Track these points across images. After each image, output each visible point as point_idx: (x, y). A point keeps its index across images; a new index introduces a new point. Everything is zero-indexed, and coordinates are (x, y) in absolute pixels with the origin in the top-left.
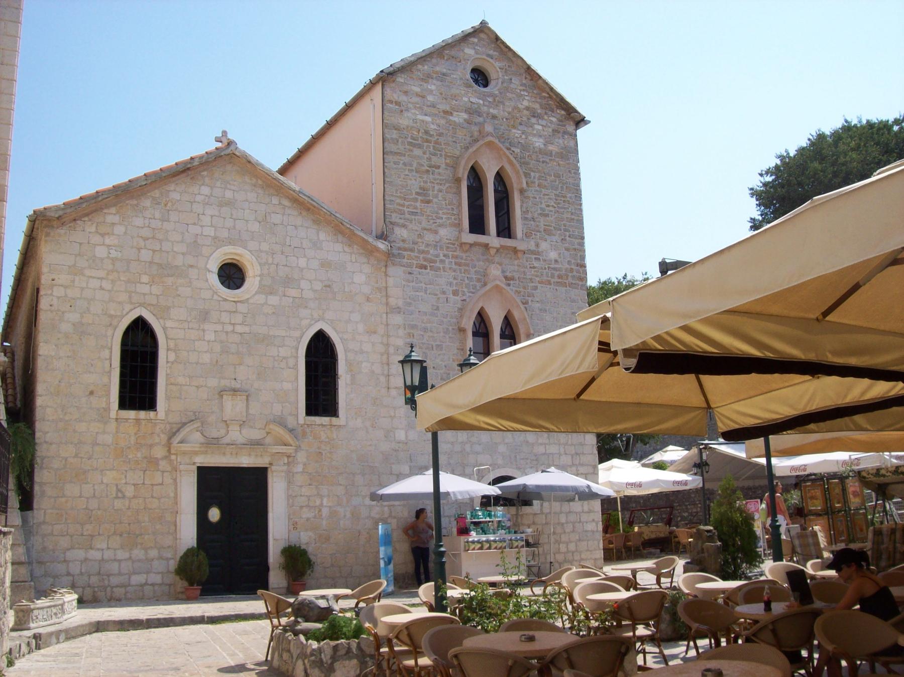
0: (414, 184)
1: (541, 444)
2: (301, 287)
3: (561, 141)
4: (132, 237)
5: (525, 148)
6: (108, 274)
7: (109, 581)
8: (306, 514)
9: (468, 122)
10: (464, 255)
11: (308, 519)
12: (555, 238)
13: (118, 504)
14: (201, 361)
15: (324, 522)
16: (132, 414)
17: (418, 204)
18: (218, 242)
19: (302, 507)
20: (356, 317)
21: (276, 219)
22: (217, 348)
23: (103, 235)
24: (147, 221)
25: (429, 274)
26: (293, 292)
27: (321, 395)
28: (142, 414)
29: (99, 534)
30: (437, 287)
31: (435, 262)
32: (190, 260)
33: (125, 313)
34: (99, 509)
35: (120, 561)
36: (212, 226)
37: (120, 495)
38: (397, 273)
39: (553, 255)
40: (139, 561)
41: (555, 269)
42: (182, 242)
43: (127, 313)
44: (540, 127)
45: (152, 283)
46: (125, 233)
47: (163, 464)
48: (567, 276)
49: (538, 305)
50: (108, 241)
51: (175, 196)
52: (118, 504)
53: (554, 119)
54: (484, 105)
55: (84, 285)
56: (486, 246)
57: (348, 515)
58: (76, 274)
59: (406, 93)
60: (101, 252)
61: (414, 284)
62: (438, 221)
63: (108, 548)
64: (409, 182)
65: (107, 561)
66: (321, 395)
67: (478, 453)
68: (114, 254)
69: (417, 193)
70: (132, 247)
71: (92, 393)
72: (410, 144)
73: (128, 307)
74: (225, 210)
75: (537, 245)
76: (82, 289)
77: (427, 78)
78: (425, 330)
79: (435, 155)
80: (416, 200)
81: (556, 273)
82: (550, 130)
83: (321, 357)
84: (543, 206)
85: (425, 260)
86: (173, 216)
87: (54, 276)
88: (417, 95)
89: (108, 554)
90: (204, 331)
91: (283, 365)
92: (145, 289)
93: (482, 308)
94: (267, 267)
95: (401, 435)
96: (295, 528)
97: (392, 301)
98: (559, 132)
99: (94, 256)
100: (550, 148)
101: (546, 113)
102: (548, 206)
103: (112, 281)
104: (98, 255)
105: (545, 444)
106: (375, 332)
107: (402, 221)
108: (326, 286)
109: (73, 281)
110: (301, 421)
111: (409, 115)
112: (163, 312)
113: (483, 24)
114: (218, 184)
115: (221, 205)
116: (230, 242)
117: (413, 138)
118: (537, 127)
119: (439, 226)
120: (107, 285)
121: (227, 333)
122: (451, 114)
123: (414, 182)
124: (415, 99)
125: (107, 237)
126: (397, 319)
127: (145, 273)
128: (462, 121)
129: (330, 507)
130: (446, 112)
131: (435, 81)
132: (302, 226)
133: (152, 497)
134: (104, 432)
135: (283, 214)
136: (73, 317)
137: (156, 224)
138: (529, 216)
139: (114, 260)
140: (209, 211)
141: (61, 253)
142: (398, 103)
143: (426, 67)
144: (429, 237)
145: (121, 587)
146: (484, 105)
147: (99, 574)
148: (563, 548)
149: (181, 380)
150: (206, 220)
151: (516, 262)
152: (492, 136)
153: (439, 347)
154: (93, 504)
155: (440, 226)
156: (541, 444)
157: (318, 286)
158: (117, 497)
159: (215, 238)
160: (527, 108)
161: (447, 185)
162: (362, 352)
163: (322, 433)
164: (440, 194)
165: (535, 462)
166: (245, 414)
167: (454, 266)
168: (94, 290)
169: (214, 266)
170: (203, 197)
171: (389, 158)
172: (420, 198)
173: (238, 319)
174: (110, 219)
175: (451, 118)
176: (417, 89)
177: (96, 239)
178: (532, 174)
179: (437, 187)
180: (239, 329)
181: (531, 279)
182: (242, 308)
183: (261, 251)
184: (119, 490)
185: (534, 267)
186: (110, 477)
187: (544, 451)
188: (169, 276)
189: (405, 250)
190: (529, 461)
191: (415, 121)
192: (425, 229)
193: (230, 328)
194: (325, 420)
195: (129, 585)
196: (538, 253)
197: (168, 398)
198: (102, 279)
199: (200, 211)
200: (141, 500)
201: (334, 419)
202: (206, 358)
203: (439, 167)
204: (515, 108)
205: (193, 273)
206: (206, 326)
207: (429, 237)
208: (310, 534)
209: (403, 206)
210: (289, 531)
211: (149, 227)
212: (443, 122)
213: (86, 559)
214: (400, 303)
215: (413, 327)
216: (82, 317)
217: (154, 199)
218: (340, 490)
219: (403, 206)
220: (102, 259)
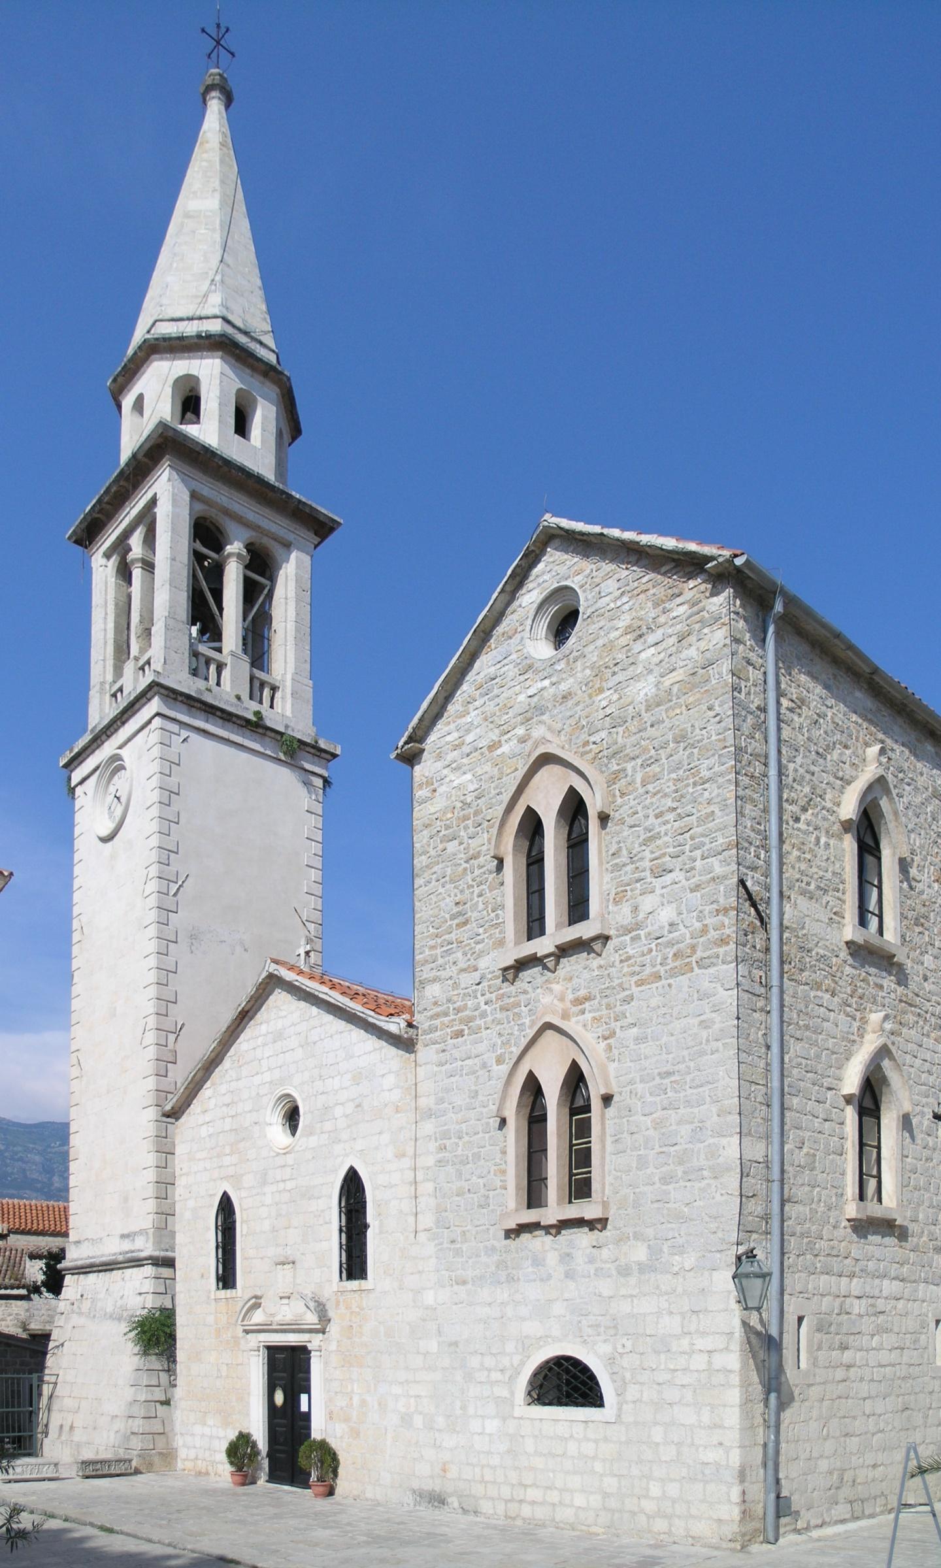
8: (341, 1402)
39: (666, 914)
49: (635, 1030)
59: (439, 757)
62: (480, 946)
64: (442, 904)
75: (635, 909)
81: (670, 952)
85: (461, 1021)
105: (632, 1296)
107: (434, 973)
119: (479, 956)
123: (448, 900)
138: (624, 858)
142: (429, 783)
144: (467, 979)
164: (481, 899)
165: (612, 1332)
181: (620, 985)
185: (628, 958)
187: (628, 1311)
189: (437, 1015)
190: (602, 1329)
192: (463, 970)
212: (487, 767)
219: (432, 948)
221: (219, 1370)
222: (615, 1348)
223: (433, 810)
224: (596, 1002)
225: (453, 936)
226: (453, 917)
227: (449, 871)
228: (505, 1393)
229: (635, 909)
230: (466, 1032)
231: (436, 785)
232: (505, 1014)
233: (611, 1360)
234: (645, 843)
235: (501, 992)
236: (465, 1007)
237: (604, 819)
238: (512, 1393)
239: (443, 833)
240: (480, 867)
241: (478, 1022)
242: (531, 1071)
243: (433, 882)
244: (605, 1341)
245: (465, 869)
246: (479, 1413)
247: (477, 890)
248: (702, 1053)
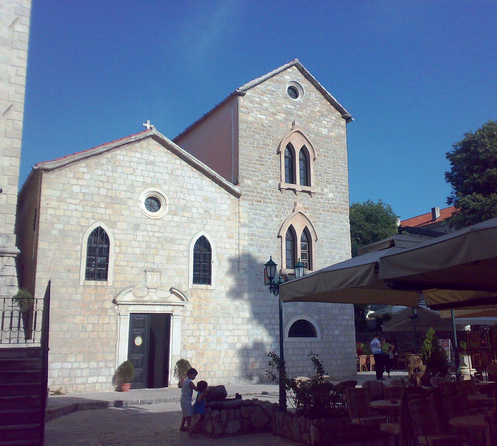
0: (256, 154)
2: (192, 211)
3: (337, 131)
4: (95, 181)
5: (317, 134)
6: (80, 202)
7: (75, 380)
8: (192, 340)
9: (285, 119)
11: (192, 344)
12: (332, 186)
13: (82, 335)
14: (134, 252)
15: (201, 345)
16: (93, 283)
17: (257, 166)
18: (145, 185)
19: (189, 336)
20: (222, 229)
21: (178, 172)
22: (144, 245)
23: (78, 179)
24: (104, 172)
25: (262, 206)
27: (202, 273)
28: (99, 283)
29: (70, 353)
30: (267, 213)
32: (129, 195)
33: (90, 224)
34: (71, 338)
35: (82, 369)
36: (142, 176)
37: (84, 330)
38: (244, 204)
39: (331, 195)
40: (94, 369)
41: (332, 204)
42: (124, 184)
43: (92, 225)
44: (326, 122)
45: (106, 208)
46: (91, 179)
47: (110, 312)
48: (339, 208)
50: (81, 182)
52: (82, 335)
53: (334, 118)
54: (295, 109)
55: (66, 208)
56: (294, 190)
57: (215, 341)
58: (61, 201)
59: (251, 102)
60: (76, 189)
61: (254, 211)
63: (76, 361)
65: (74, 369)
66: (202, 273)
68: (84, 190)
69: (257, 160)
70: (95, 187)
71: (69, 271)
72: (253, 131)
73: (92, 221)
74: (150, 167)
75: (322, 190)
76: (65, 210)
77: (264, 93)
78: (260, 237)
80: (256, 164)
83: (203, 251)
84: (326, 168)
85: (260, 197)
86: (120, 169)
87: (48, 202)
88: (258, 104)
89: (75, 365)
90: (136, 235)
91: (181, 255)
92: (102, 211)
93: (291, 225)
94: (173, 200)
96: (184, 349)
97: (242, 220)
98: (336, 125)
99: (72, 191)
100: (331, 134)
101: (329, 114)
102: (329, 168)
103: (83, 205)
104: (74, 191)
106: (232, 238)
107: (248, 176)
108: (205, 211)
109: (59, 206)
110: (190, 287)
111: (253, 114)
112: (113, 224)
114: (145, 152)
115: (147, 164)
116: (153, 185)
117: (254, 128)
118: (324, 122)
120: (80, 208)
121: (150, 236)
124: (256, 106)
125: (80, 180)
126: (245, 230)
127: (103, 202)
128: (282, 118)
129: (205, 336)
131: (267, 95)
132: (193, 177)
133: (103, 331)
134: (76, 293)
135: (183, 170)
136: (60, 226)
137: (109, 173)
139: (84, 194)
140: (141, 167)
141: (53, 189)
142: (246, 108)
144: (263, 185)
145: (82, 384)
146: (295, 109)
147: (69, 377)
148: (334, 364)
149: (123, 263)
150: (138, 172)
152: (299, 127)
153: (267, 246)
154: (68, 336)
155: (270, 178)
157: (202, 211)
158: (82, 331)
159: (144, 182)
160: (319, 111)
161: (273, 155)
162: (225, 248)
163: (202, 294)
166: (158, 283)
167: (276, 201)
168: (72, 211)
169: (143, 198)
170: (136, 159)
173: (157, 229)
174: (82, 170)
177: (74, 181)
178: (321, 149)
179: (267, 157)
180: (157, 235)
182: (159, 223)
183: (170, 191)
184: (83, 327)
185: (320, 202)
186: (78, 319)
188: (116, 204)
189: (249, 191)
191: (256, 118)
193: (151, 234)
194: (204, 286)
195: (87, 383)
196: (323, 195)
197: (115, 273)
198: (76, 205)
199: (135, 167)
200: (96, 333)
201: (209, 285)
202: (137, 251)
203: (268, 145)
204: (312, 111)
205: (131, 203)
206: (138, 233)
208: (193, 352)
209: (249, 167)
210: (181, 351)
211: (105, 175)
212: (272, 119)
213: (62, 368)
214: (246, 221)
215: (253, 235)
216: (64, 226)
217: (108, 159)
218: (211, 327)
219: (249, 167)
220: (77, 193)
222: (320, 318)
225: (257, 166)
226: (257, 160)
227: (256, 144)
229: (322, 190)
233: (319, 322)
234: (325, 173)
236: (262, 193)
239: (253, 129)
240: (269, 149)
243: (248, 144)
248: (341, 237)
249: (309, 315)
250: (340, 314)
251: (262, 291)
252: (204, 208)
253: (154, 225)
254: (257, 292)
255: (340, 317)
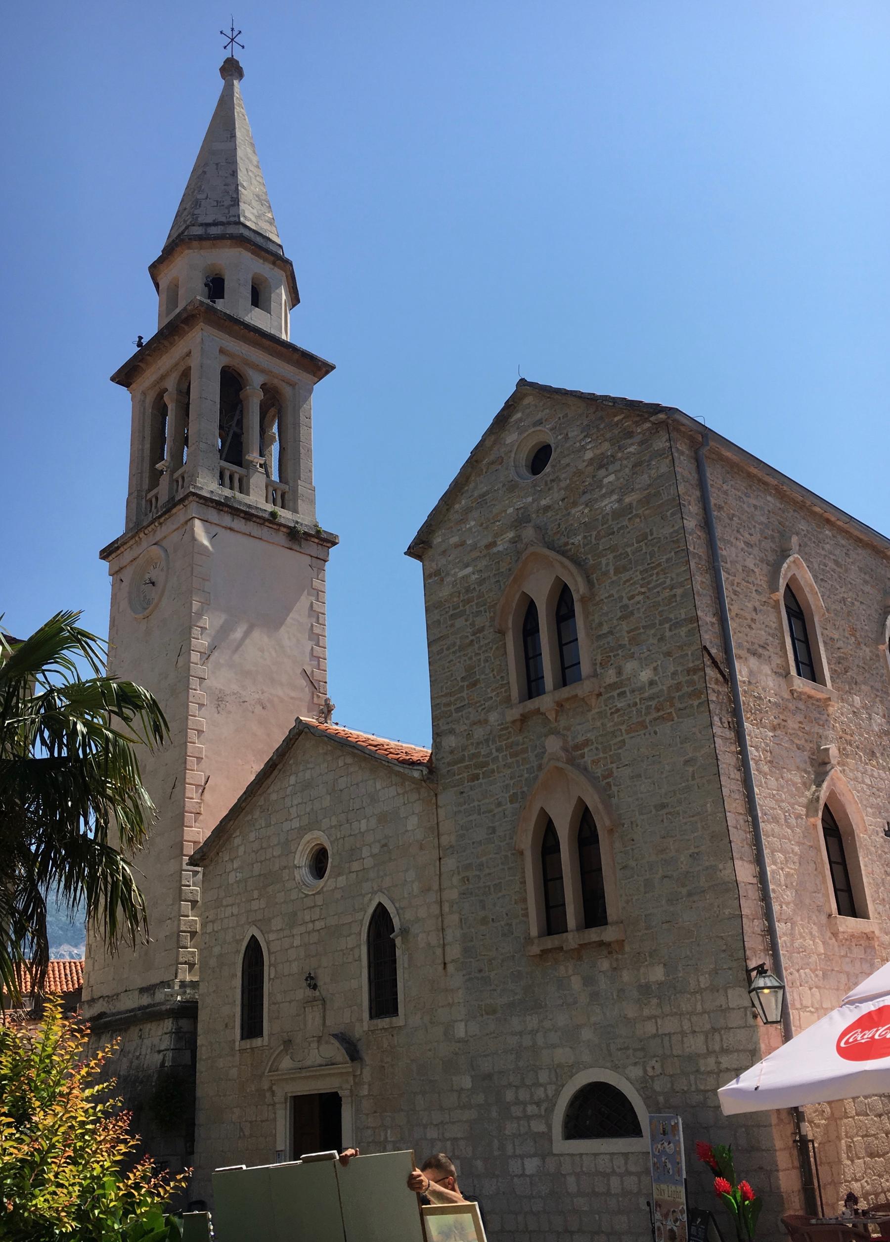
1: (649, 1018)
10: (520, 738)
17: (464, 694)
20: (411, 875)
21: (342, 783)
26: (356, 866)
31: (486, 764)
39: (645, 675)
41: (651, 698)
51: (274, 797)
53: (632, 449)
67: (554, 1046)
75: (619, 673)
78: (481, 866)
79: (478, 613)
80: (462, 689)
82: (627, 470)
84: (625, 601)
95: (460, 1031)
100: (627, 500)
105: (655, 1017)
106: (429, 889)
111: (449, 579)
113: (522, 382)
118: (606, 481)
119: (488, 711)
122: (493, 544)
130: (489, 546)
143: (463, 502)
150: (293, 810)
151: (590, 715)
155: (490, 709)
156: (649, 1018)
157: (376, 850)
164: (487, 664)
167: (510, 760)
171: (436, 648)
172: (466, 683)
175: (495, 550)
176: (455, 540)
181: (613, 732)
187: (654, 1031)
189: (456, 763)
197: (270, 1021)
203: (481, 630)
207: (479, 733)
215: (468, 867)
217: (261, 806)
221: (241, 1129)
222: (645, 1071)
223: (441, 595)
224: (593, 747)
228: (541, 1128)
229: (619, 673)
230: (481, 776)
231: (443, 575)
232: (514, 760)
233: (644, 1086)
235: (510, 740)
237: (583, 600)
238: (550, 1127)
239: (451, 612)
241: (491, 766)
242: (542, 808)
243: (445, 652)
244: (635, 1064)
245: (472, 641)
246: (518, 1152)
247: (482, 657)
249: (615, 1068)
250: (710, 1053)
251: (494, 1012)
252: (379, 841)
253: (313, 907)
254: (485, 1017)
255: (711, 1061)
